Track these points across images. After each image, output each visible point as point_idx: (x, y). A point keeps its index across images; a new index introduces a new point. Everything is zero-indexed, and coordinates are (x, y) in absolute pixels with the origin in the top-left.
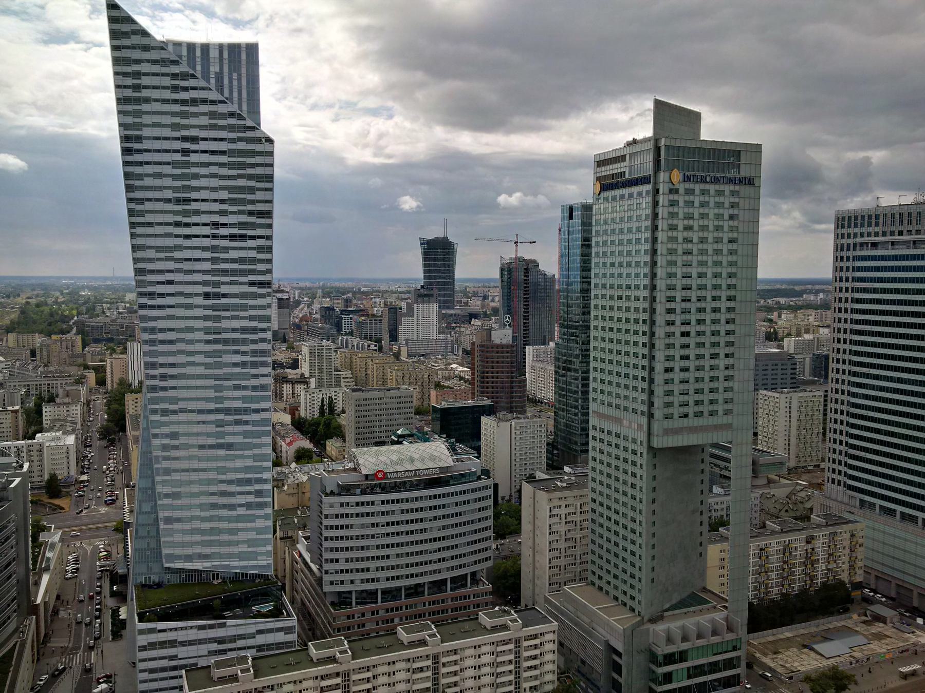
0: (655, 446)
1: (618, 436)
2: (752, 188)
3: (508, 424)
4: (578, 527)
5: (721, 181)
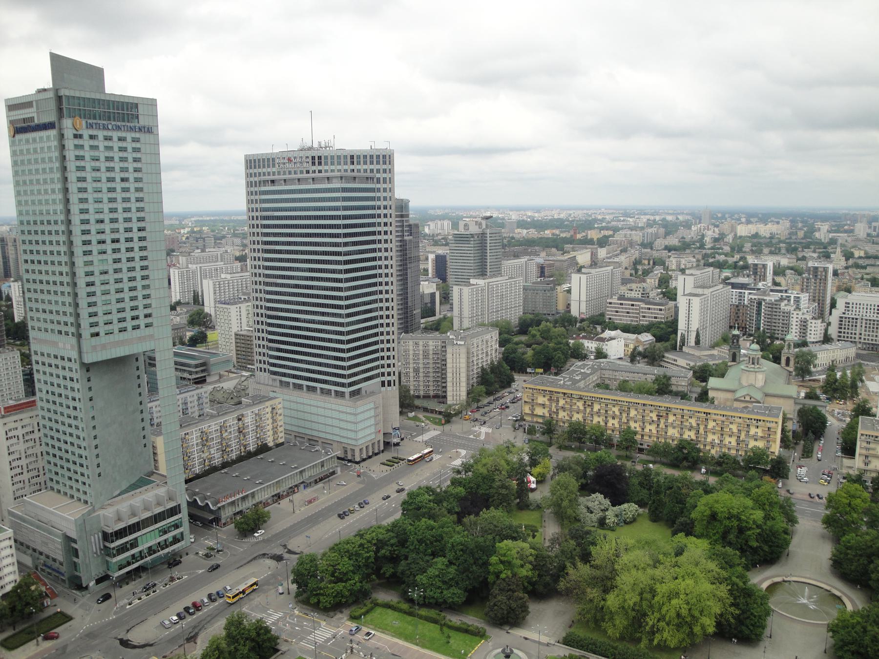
2: (152, 136)
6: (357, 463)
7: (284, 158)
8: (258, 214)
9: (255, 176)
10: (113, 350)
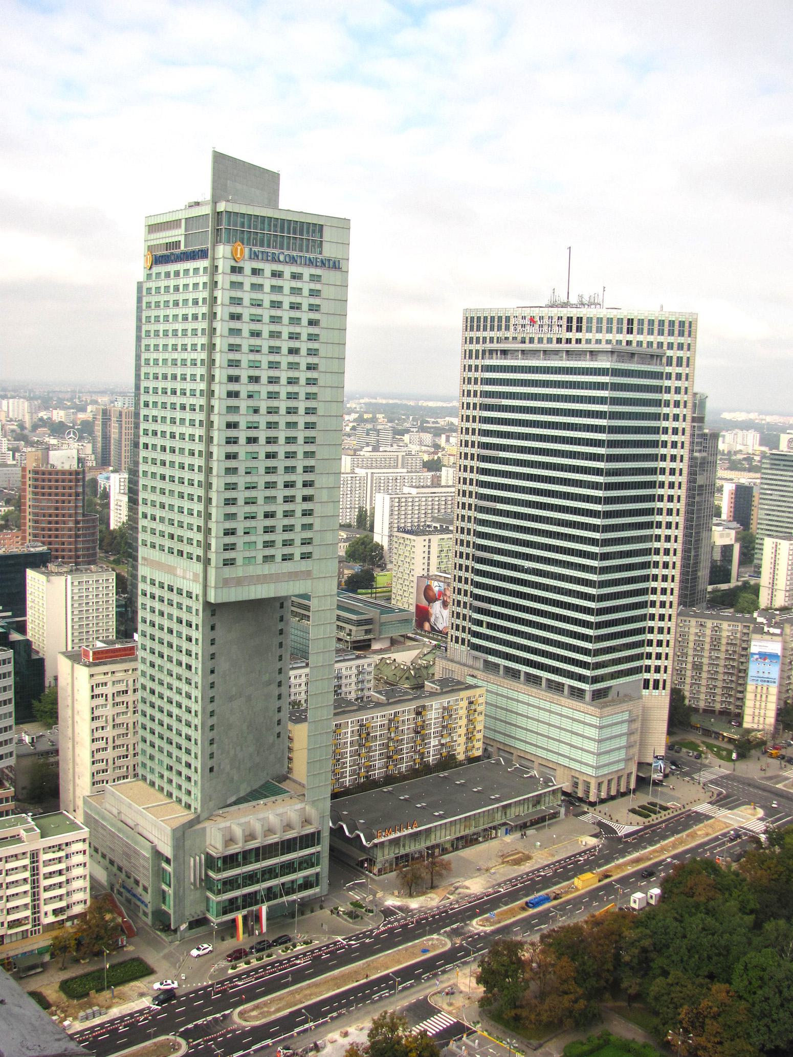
0: (213, 601)
1: (171, 589)
2: (338, 273)
3: (63, 578)
4: (131, 709)
5: (298, 262)
6: (592, 804)
7: (524, 318)
8: (478, 400)
9: (478, 342)
10: (253, 588)
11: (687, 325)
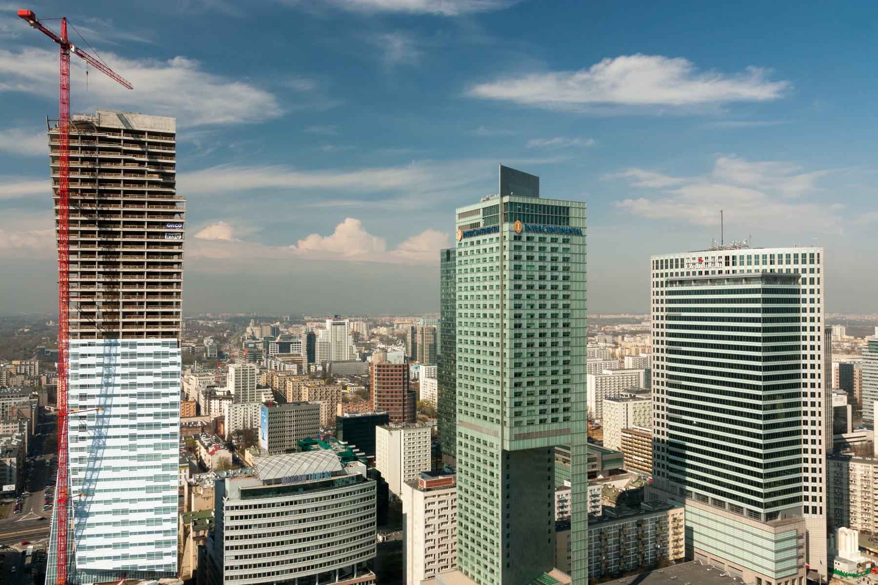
1: (479, 441)
3: (399, 432)
7: (694, 259)
9: (662, 276)
11: (816, 256)
